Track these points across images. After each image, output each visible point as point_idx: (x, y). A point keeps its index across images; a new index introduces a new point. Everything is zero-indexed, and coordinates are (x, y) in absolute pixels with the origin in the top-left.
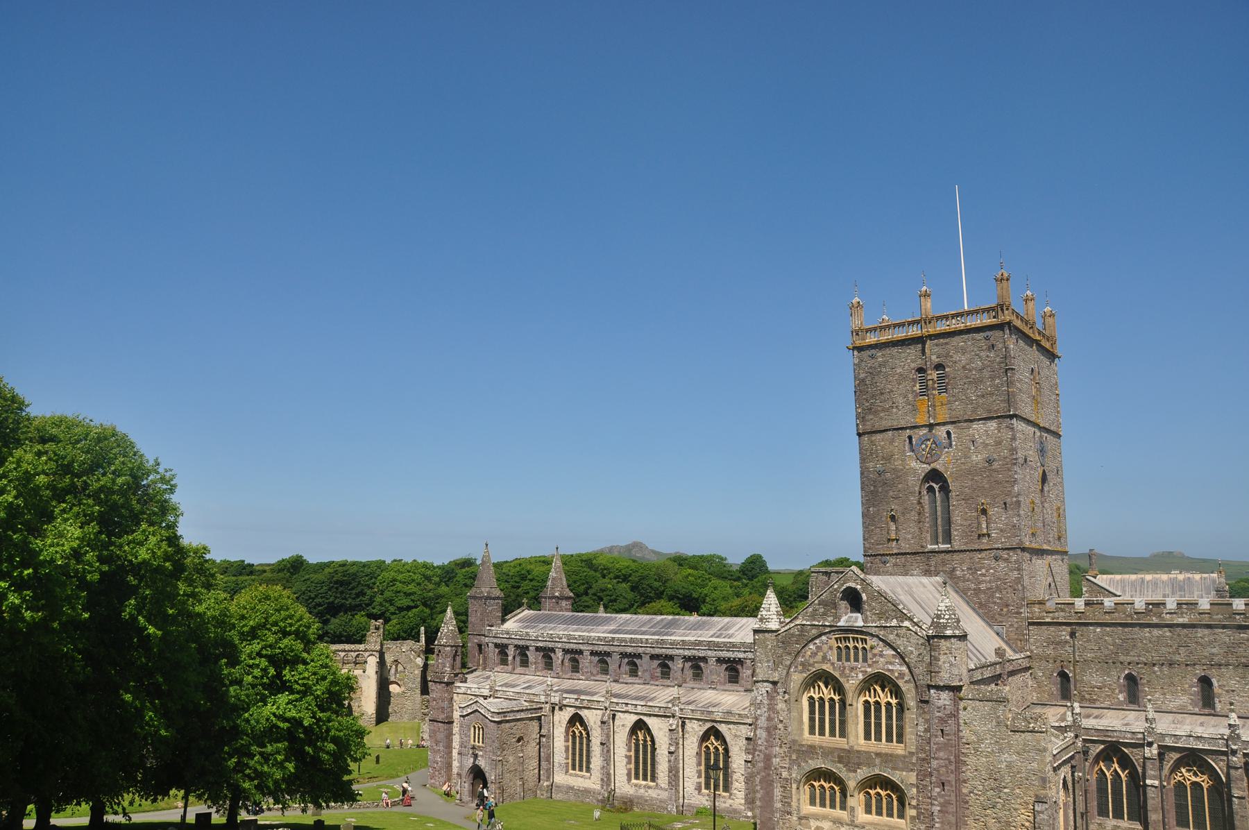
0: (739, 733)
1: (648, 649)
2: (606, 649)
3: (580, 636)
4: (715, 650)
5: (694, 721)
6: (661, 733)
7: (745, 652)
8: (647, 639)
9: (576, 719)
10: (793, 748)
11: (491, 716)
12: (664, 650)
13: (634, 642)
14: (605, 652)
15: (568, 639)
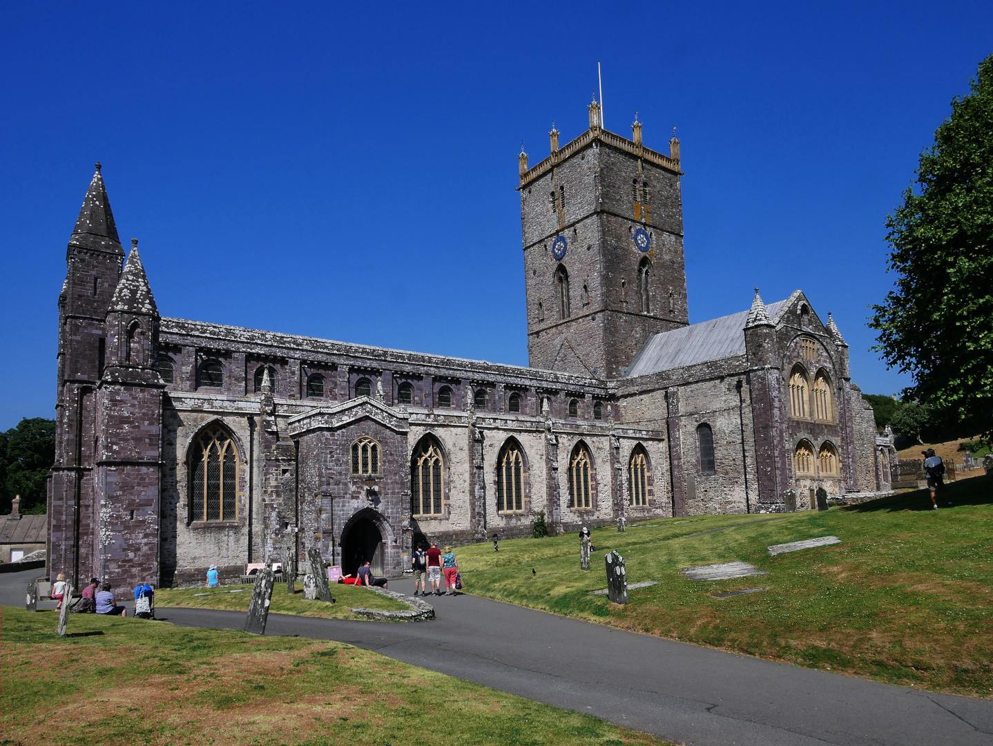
0: (601, 446)
1: (432, 369)
2: (375, 364)
3: (333, 345)
4: (505, 376)
5: (563, 435)
6: (533, 451)
7: (531, 379)
8: (430, 358)
9: (429, 441)
10: (791, 424)
11: (396, 426)
12: (451, 372)
13: (414, 359)
14: (372, 368)
15: (313, 347)
